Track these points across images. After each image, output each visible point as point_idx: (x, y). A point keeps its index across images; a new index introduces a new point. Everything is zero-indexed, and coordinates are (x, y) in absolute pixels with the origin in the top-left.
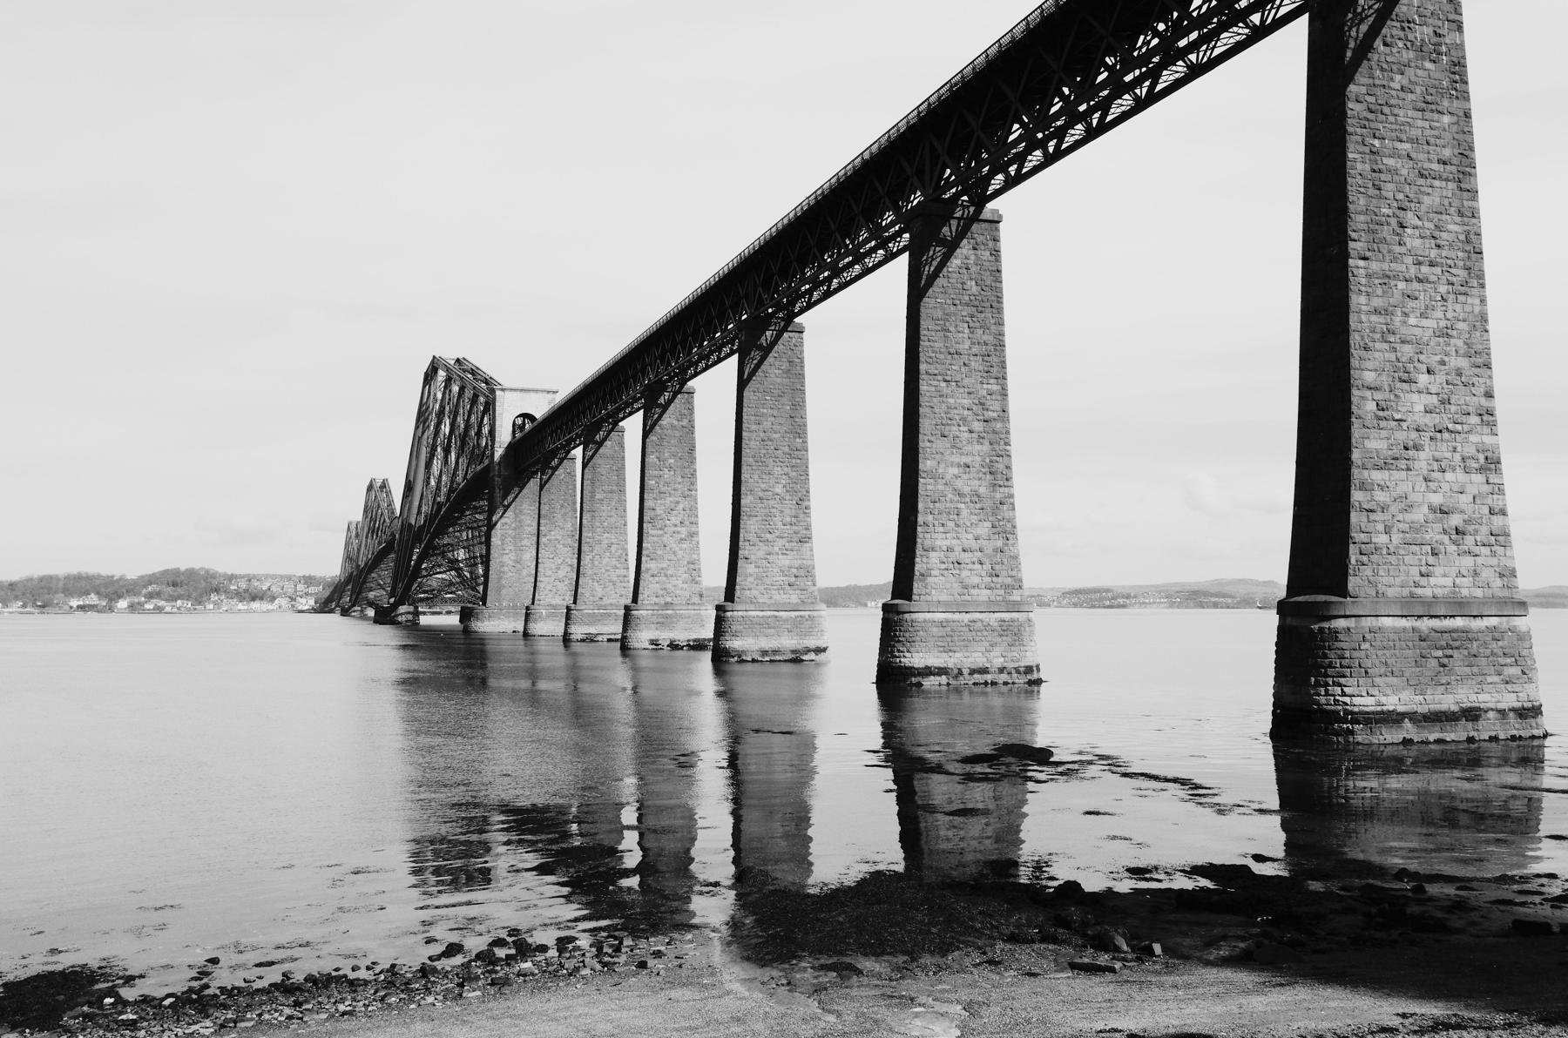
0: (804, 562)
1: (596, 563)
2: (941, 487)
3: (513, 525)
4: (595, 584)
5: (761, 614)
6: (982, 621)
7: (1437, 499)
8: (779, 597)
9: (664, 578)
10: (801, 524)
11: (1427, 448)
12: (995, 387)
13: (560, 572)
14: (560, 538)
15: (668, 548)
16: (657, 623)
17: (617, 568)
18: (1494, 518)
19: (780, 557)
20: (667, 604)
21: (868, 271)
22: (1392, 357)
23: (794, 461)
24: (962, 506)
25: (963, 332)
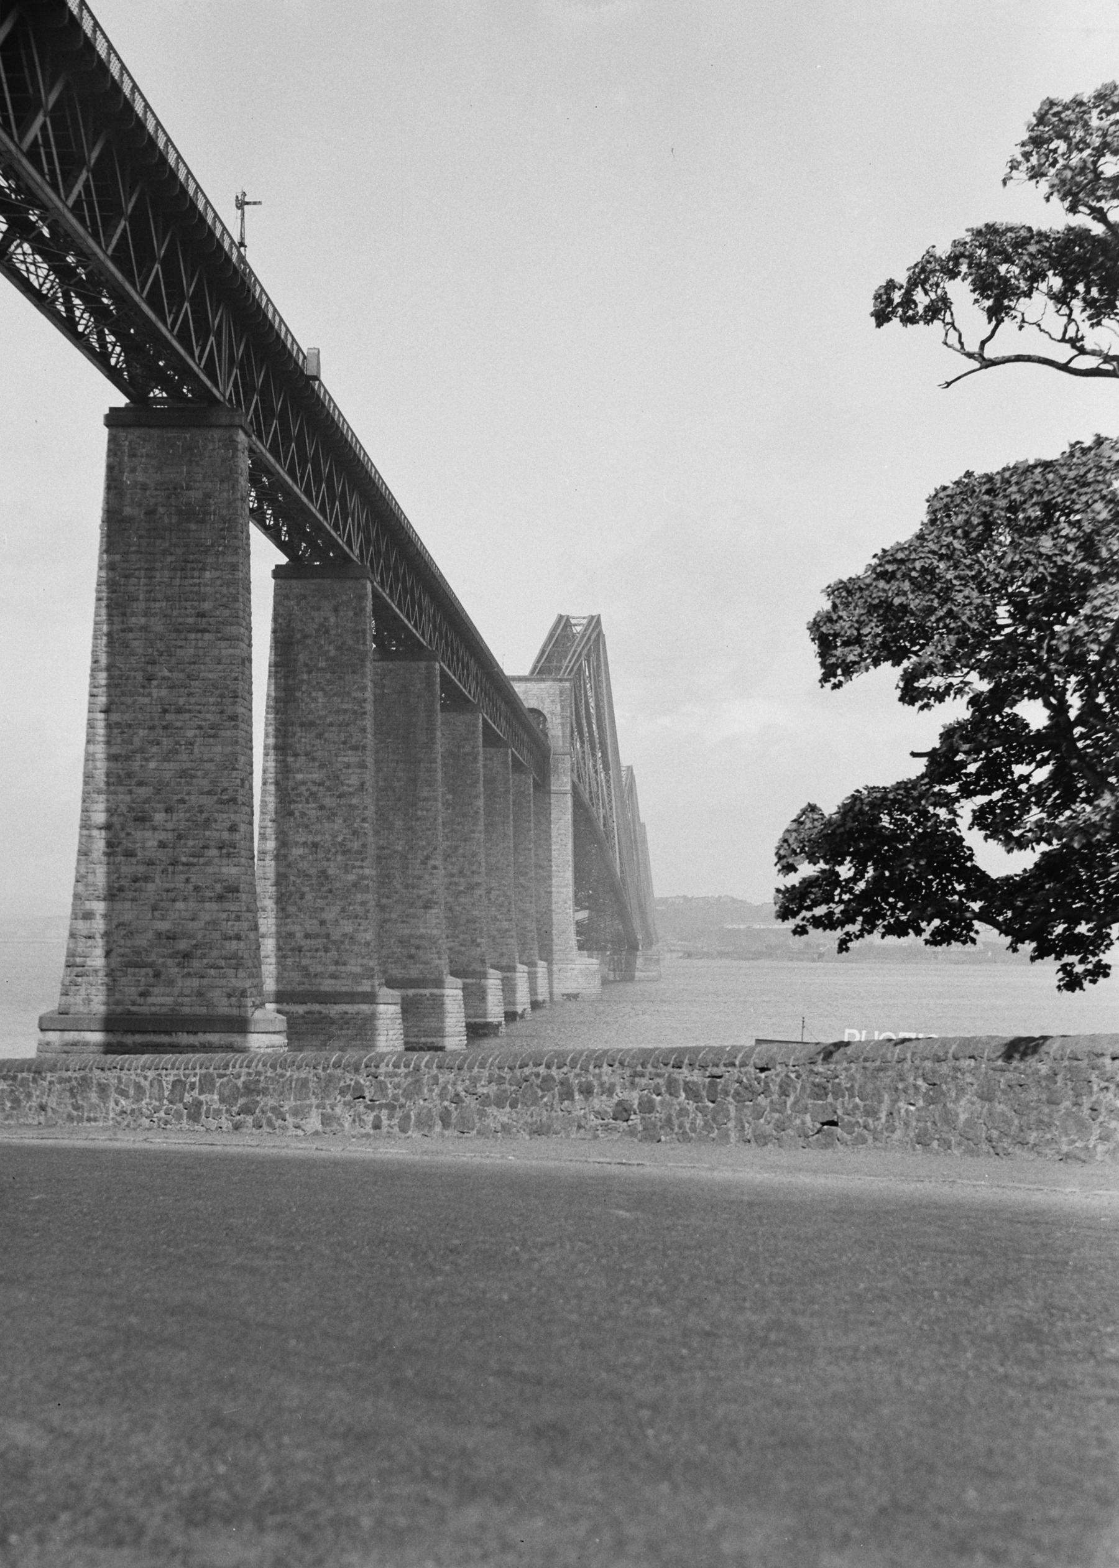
7: (164, 926)
11: (157, 880)
18: (227, 943)
19: (398, 925)
22: (128, 798)
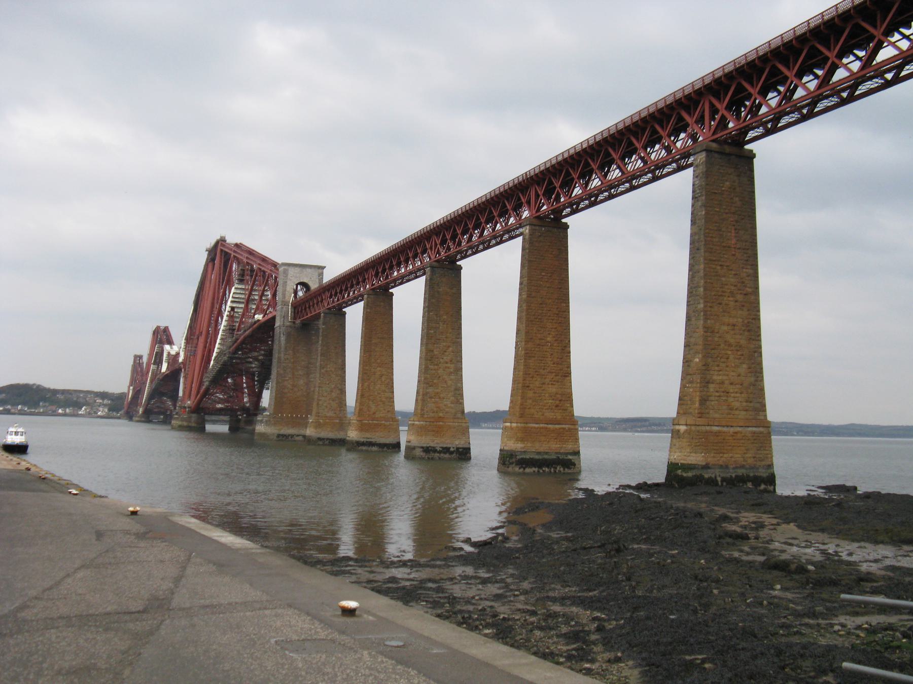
0: (566, 390)
1: (372, 388)
2: (716, 339)
3: (292, 360)
4: (371, 402)
5: (537, 426)
6: (741, 433)
8: (549, 415)
9: (438, 400)
10: (564, 363)
12: (751, 271)
13: (333, 394)
14: (333, 370)
15: (441, 378)
16: (434, 431)
17: (386, 392)
19: (550, 386)
20: (441, 417)
21: (633, 188)
23: (560, 319)
24: (730, 352)
25: (730, 232)
